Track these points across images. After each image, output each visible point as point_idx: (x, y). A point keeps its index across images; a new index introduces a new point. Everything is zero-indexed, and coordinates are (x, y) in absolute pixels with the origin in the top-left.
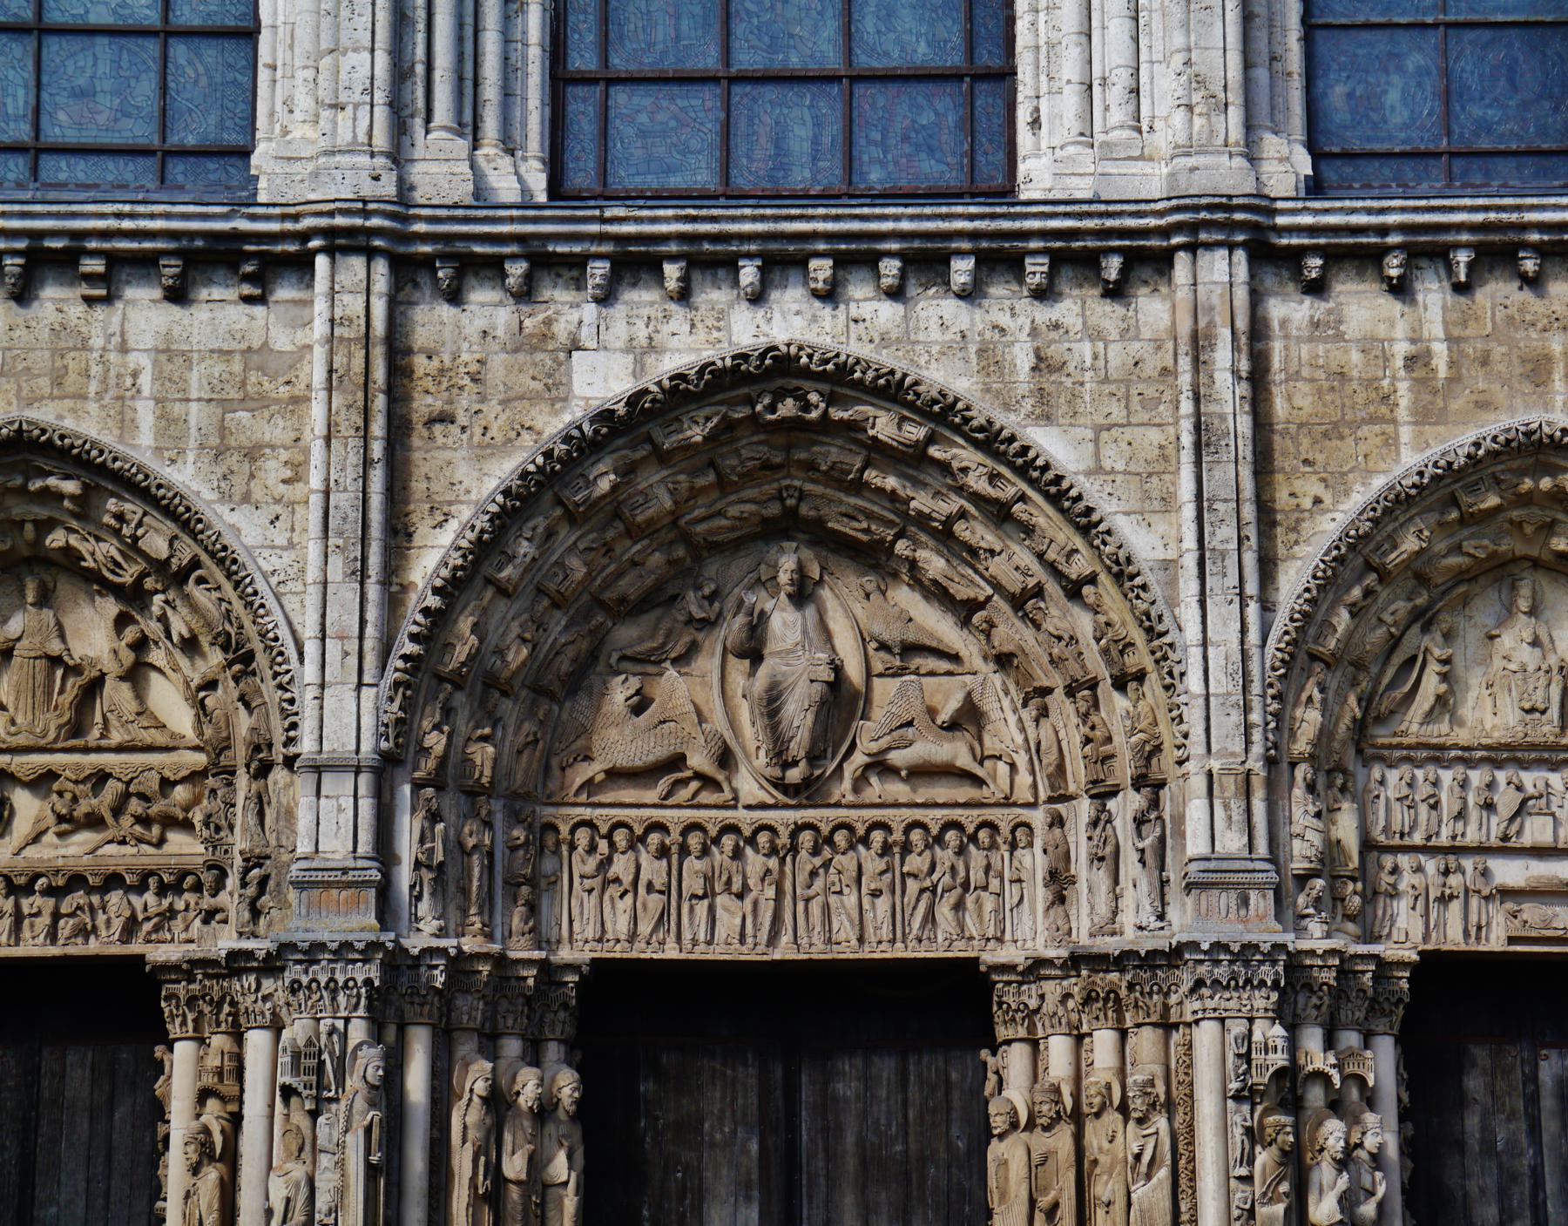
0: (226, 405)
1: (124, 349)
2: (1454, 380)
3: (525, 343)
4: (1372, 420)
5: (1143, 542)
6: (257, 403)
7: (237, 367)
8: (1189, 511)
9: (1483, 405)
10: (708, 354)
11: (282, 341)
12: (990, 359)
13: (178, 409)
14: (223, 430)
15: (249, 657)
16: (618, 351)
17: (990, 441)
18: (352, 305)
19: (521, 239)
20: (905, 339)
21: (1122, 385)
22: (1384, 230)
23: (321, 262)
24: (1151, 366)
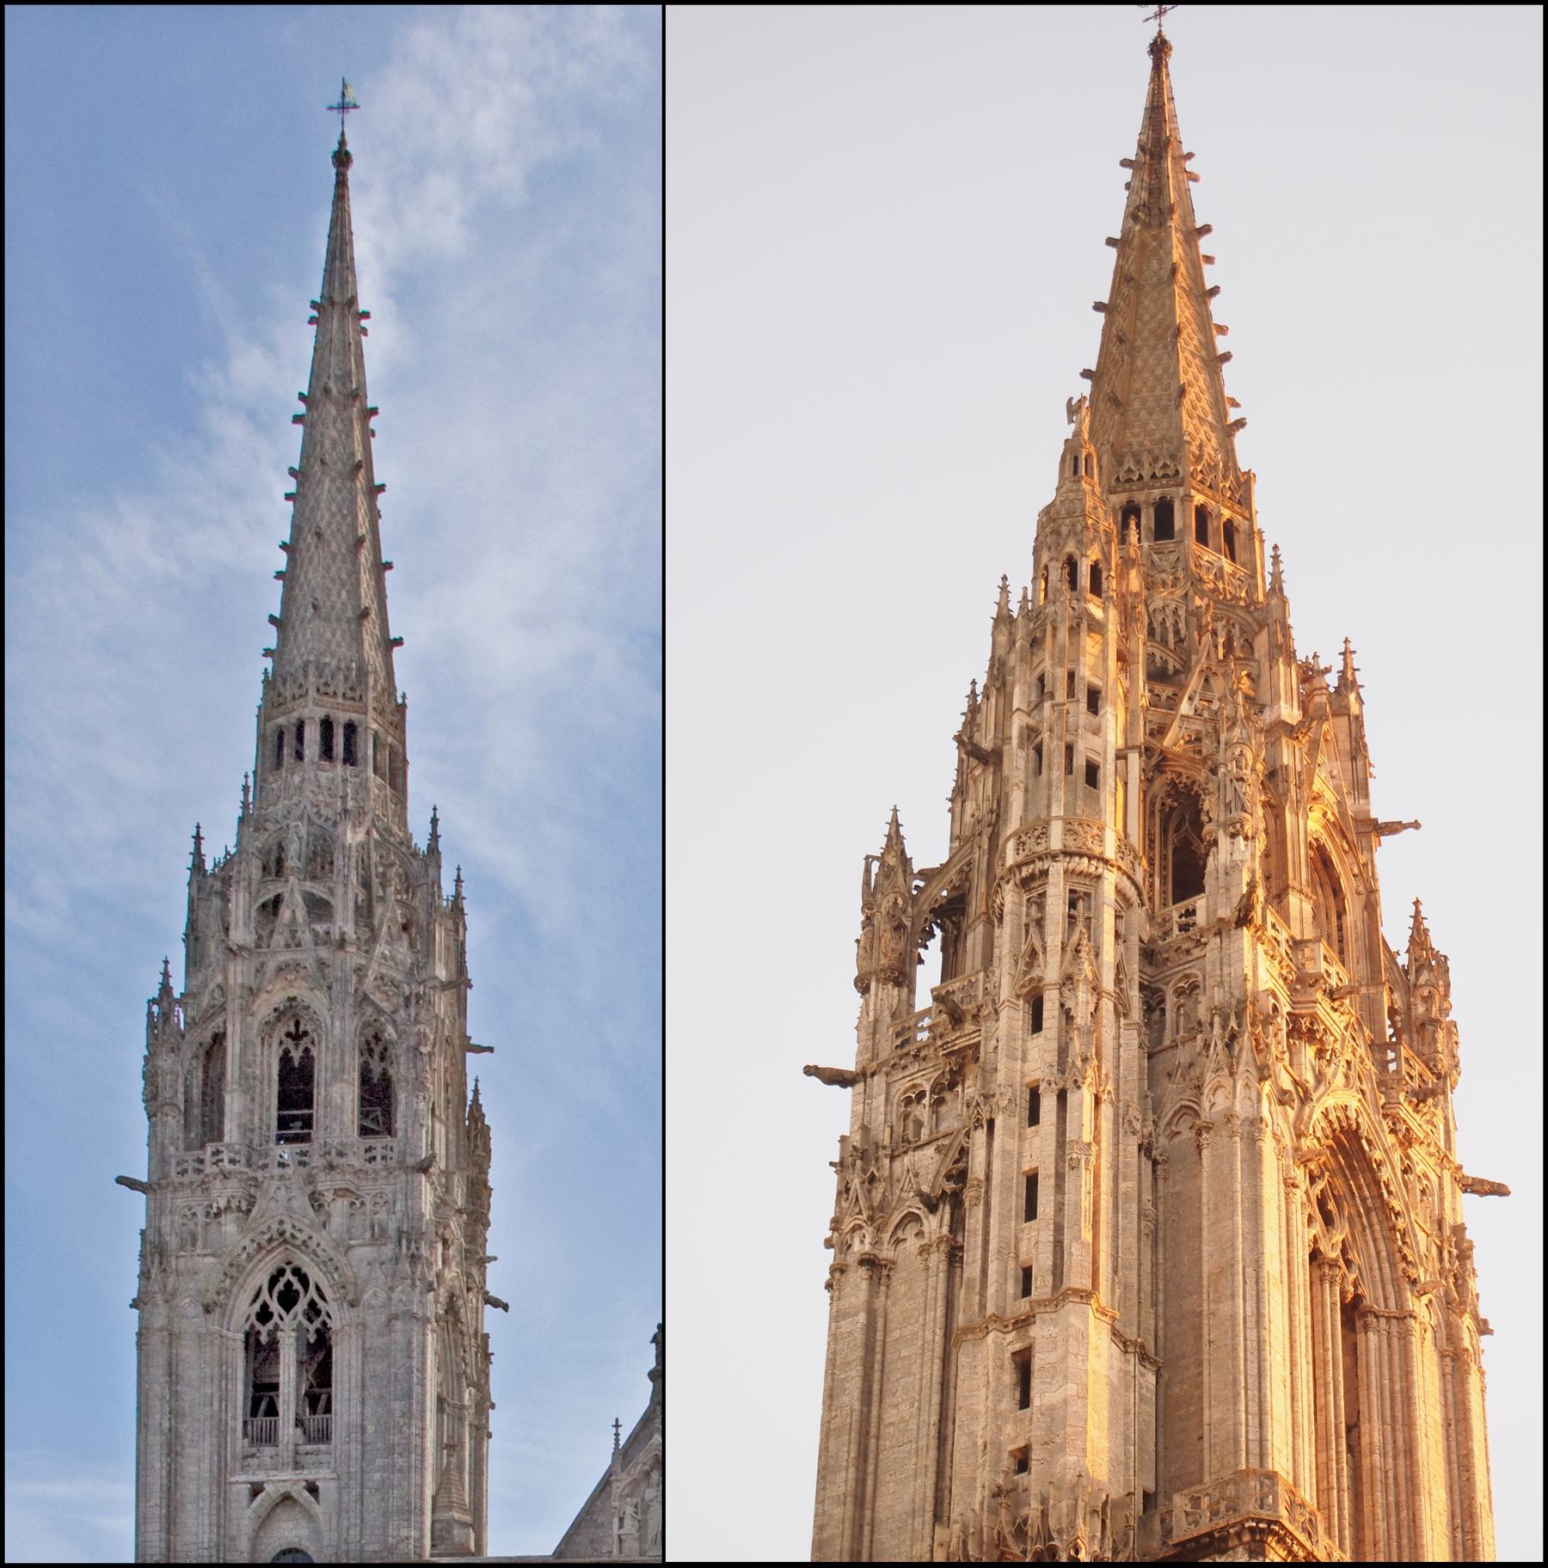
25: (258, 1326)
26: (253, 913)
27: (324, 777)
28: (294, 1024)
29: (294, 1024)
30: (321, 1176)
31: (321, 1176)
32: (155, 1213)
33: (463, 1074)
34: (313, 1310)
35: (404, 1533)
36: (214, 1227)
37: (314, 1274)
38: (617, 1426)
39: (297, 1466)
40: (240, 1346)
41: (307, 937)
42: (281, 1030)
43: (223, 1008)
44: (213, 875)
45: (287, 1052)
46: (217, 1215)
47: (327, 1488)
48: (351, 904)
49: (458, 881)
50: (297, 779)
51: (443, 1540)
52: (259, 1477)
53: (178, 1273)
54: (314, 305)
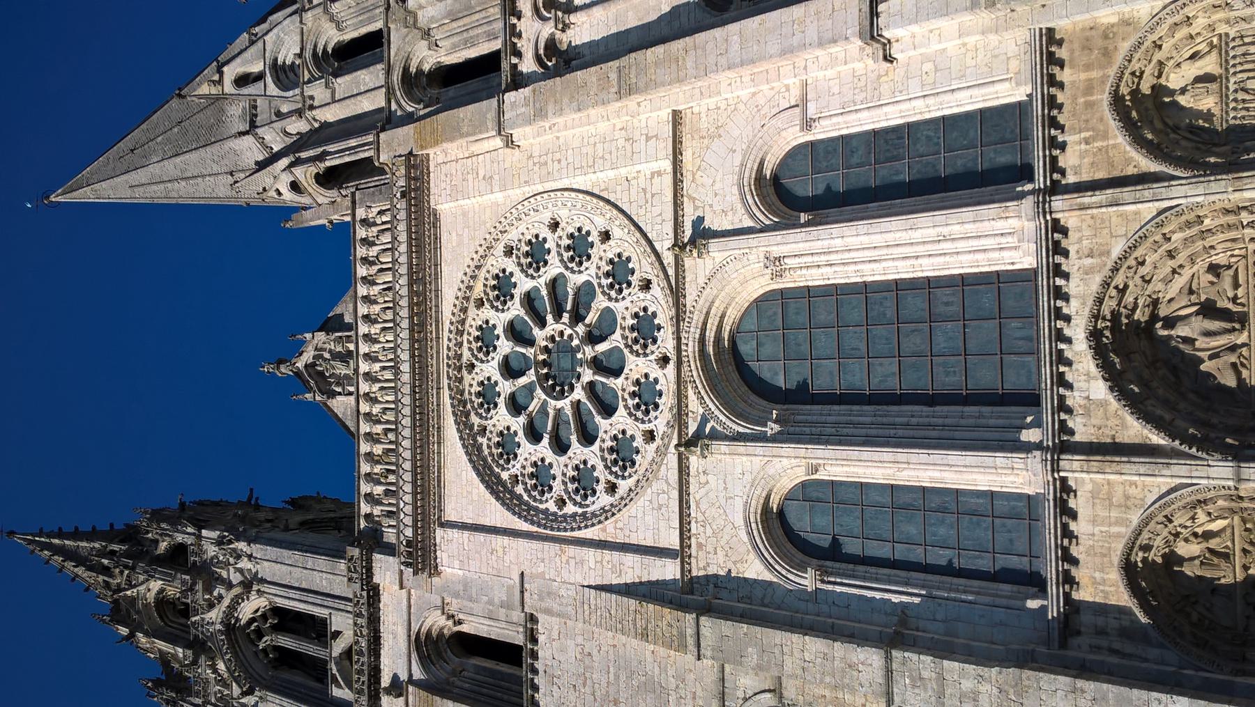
0: (1111, 505)
1: (1093, 535)
2: (1093, 129)
3: (1088, 414)
4: (1107, 152)
6: (1109, 498)
7: (1097, 501)
8: (1139, 206)
9: (1102, 119)
10: (1090, 357)
11: (1089, 487)
12: (1088, 271)
13: (1113, 520)
14: (1120, 506)
15: (1199, 501)
16: (1089, 385)
17: (1115, 269)
18: (1076, 465)
19: (1053, 414)
20: (1083, 298)
21: (1096, 232)
22: (1045, 156)
23: (1062, 474)
24: (1091, 222)
34: (264, 617)
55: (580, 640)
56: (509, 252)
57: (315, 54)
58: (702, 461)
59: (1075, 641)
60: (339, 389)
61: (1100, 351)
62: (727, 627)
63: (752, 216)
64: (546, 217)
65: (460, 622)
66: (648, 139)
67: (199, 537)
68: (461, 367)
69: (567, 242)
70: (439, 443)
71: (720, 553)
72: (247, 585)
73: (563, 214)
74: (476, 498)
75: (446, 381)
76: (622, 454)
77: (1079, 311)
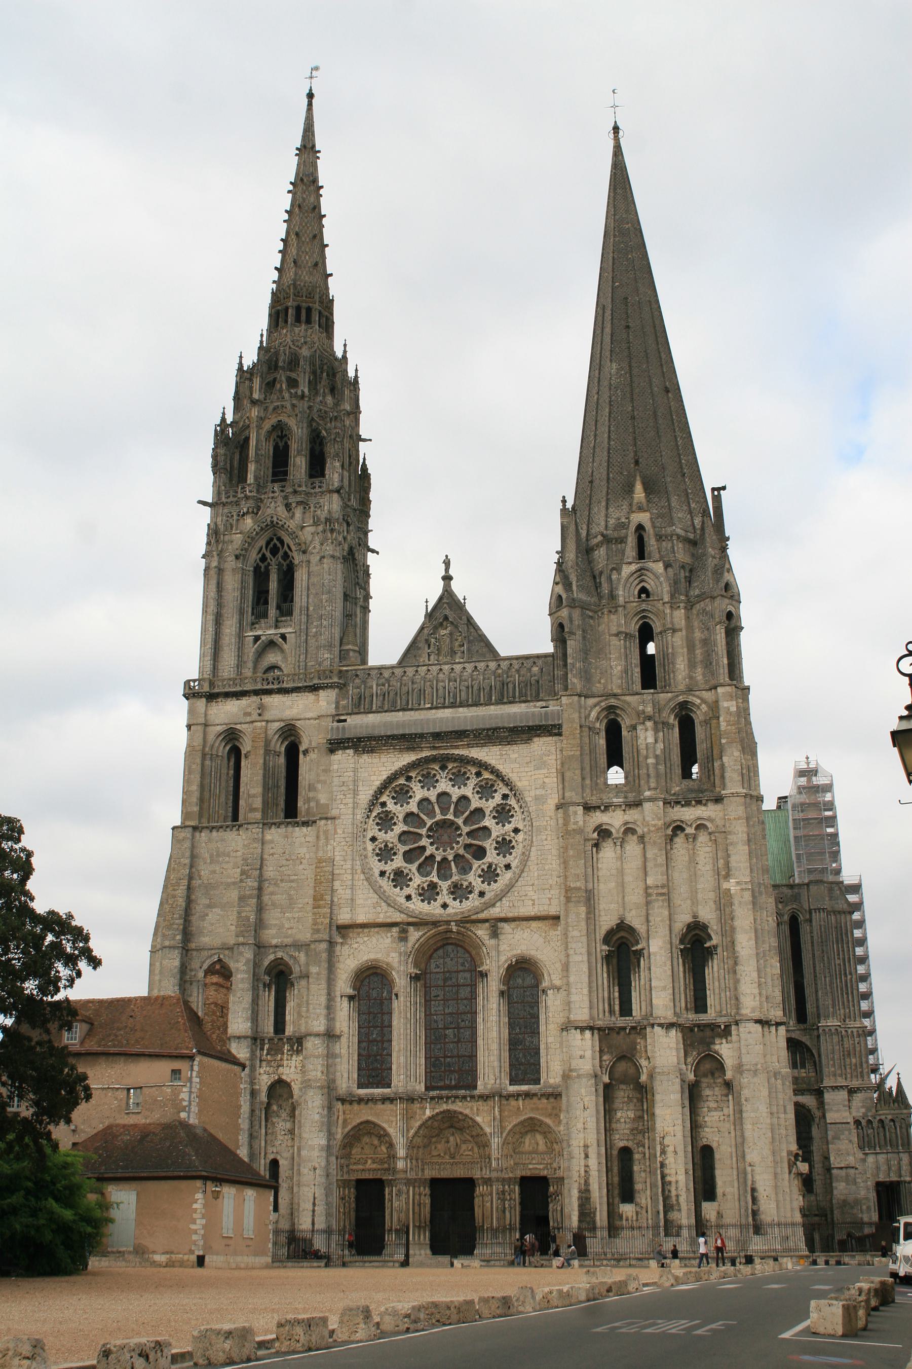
3: (421, 1108)
5: (488, 1130)
12: (472, 1109)
17: (471, 1118)
25: (260, 564)
26: (264, 386)
27: (297, 330)
28: (280, 433)
29: (280, 433)
30: (291, 496)
31: (291, 496)
32: (214, 516)
33: (358, 451)
34: (286, 556)
35: (326, 656)
36: (241, 521)
37: (287, 539)
38: (427, 602)
39: (276, 627)
40: (251, 574)
41: (287, 395)
42: (274, 436)
43: (249, 426)
44: (246, 372)
45: (277, 443)
46: (243, 515)
47: (291, 638)
48: (307, 380)
49: (356, 370)
50: (285, 331)
51: (345, 659)
52: (259, 633)
53: (224, 542)
54: (297, 149)
55: (307, 856)
56: (505, 797)
57: (644, 610)
58: (396, 935)
59: (339, 1103)
60: (432, 646)
61: (444, 1112)
62: (324, 955)
63: (506, 961)
64: (520, 827)
65: (304, 754)
66: (550, 899)
67: (331, 492)
68: (443, 762)
69: (508, 838)
70: (401, 750)
71: (356, 946)
72: (304, 552)
73: (520, 837)
74: (373, 778)
75: (434, 753)
76: (400, 878)
77: (458, 1106)
